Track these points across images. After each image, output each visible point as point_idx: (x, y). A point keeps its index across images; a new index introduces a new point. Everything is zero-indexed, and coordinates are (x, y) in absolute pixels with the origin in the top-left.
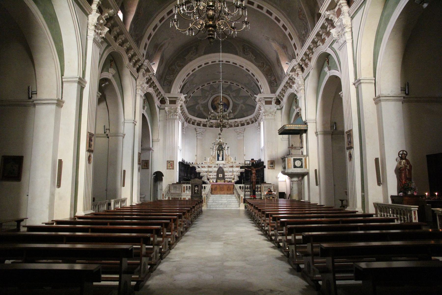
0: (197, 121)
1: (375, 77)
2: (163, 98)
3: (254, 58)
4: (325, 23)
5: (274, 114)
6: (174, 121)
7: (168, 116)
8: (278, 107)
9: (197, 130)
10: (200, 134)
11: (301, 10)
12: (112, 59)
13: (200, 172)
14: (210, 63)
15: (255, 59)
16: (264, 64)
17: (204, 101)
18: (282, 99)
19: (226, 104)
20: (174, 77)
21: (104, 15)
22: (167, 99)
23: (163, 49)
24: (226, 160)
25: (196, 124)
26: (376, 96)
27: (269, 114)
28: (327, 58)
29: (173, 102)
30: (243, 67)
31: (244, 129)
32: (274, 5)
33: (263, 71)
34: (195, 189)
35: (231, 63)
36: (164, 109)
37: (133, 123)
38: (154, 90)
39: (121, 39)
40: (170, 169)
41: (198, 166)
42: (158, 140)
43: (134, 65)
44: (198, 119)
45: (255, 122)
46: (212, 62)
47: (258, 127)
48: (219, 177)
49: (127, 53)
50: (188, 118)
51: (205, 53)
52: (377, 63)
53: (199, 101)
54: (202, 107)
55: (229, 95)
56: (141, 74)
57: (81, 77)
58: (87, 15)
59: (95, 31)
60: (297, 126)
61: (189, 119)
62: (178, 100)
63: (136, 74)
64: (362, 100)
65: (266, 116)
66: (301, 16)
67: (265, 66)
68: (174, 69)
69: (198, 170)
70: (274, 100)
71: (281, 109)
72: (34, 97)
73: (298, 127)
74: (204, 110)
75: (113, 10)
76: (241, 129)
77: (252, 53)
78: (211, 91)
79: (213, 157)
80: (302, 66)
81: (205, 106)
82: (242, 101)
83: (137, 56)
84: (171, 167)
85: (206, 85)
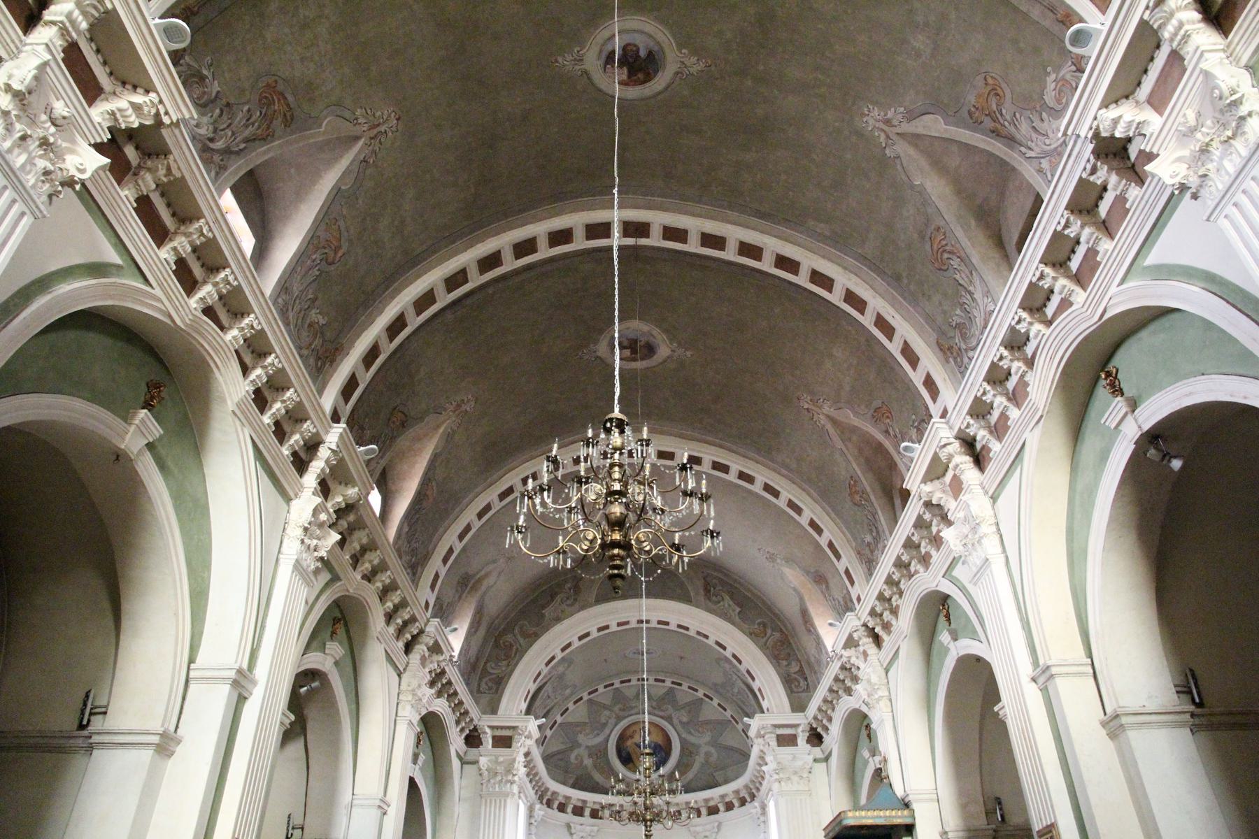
0: (574, 802)
1: (1090, 656)
2: (475, 729)
3: (738, 609)
4: (924, 513)
6: (505, 801)
7: (487, 786)
8: (816, 751)
9: (573, 831)
11: (855, 481)
12: (339, 615)
14: (614, 628)
15: (739, 613)
16: (765, 625)
17: (595, 737)
18: (826, 729)
19: (660, 746)
20: (508, 665)
21: (333, 499)
22: (485, 733)
23: (483, 588)
25: (570, 809)
26: (1105, 714)
27: (792, 777)
28: (944, 605)
29: (503, 741)
30: (706, 637)
31: (716, 824)
32: (783, 471)
33: (763, 648)
35: (673, 627)
36: (476, 762)
37: (379, 807)
38: (450, 707)
39: (370, 562)
43: (400, 632)
44: (577, 795)
45: (749, 800)
46: (619, 624)
47: (762, 819)
49: (381, 600)
50: (547, 789)
51: (602, 599)
52: (1087, 617)
53: (581, 738)
54: (590, 756)
55: (669, 719)
56: (415, 657)
57: (245, 666)
58: (288, 500)
59: (303, 541)
60: (882, 813)
61: (549, 793)
62: (520, 734)
63: (401, 659)
64: (1067, 728)
65: (783, 783)
66: (857, 497)
67: (769, 632)
68: (511, 645)
70: (803, 731)
71: (827, 759)
72: (97, 723)
73: (886, 817)
74: (595, 766)
75: (356, 489)
76: (708, 827)
77: (732, 598)
78: (616, 709)
80: (876, 631)
81: (599, 753)
82: (707, 737)
83: (409, 609)
85: (601, 689)
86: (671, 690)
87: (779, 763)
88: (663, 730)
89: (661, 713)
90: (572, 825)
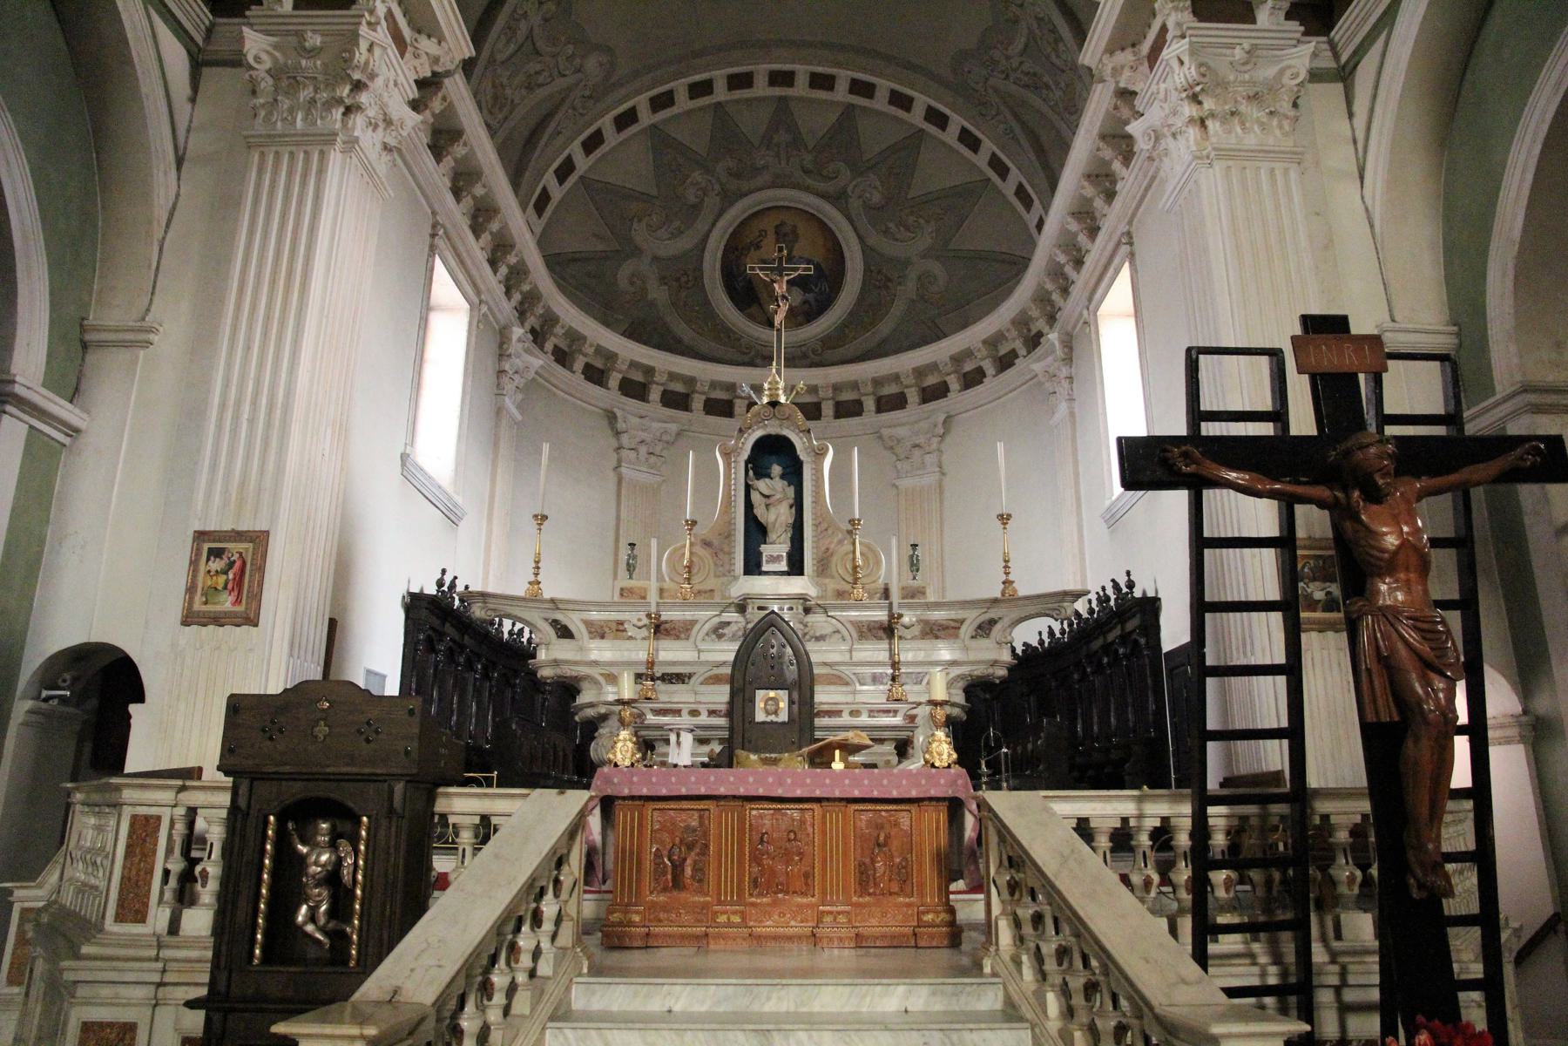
5: (1285, 106)
9: (621, 425)
10: (643, 450)
13: (569, 671)
17: (673, 236)
24: (823, 567)
27: (1243, 108)
31: (942, 417)
34: (289, 866)
40: (218, 620)
41: (555, 623)
42: (137, 338)
45: (1023, 352)
47: (1064, 372)
48: (760, 717)
53: (640, 233)
54: (663, 280)
69: (551, 657)
76: (924, 425)
78: (720, 168)
79: (707, 544)
84: (226, 603)
85: (683, 103)
86: (849, 110)
87: (1201, 65)
88: (823, 227)
89: (823, 186)
90: (619, 413)
